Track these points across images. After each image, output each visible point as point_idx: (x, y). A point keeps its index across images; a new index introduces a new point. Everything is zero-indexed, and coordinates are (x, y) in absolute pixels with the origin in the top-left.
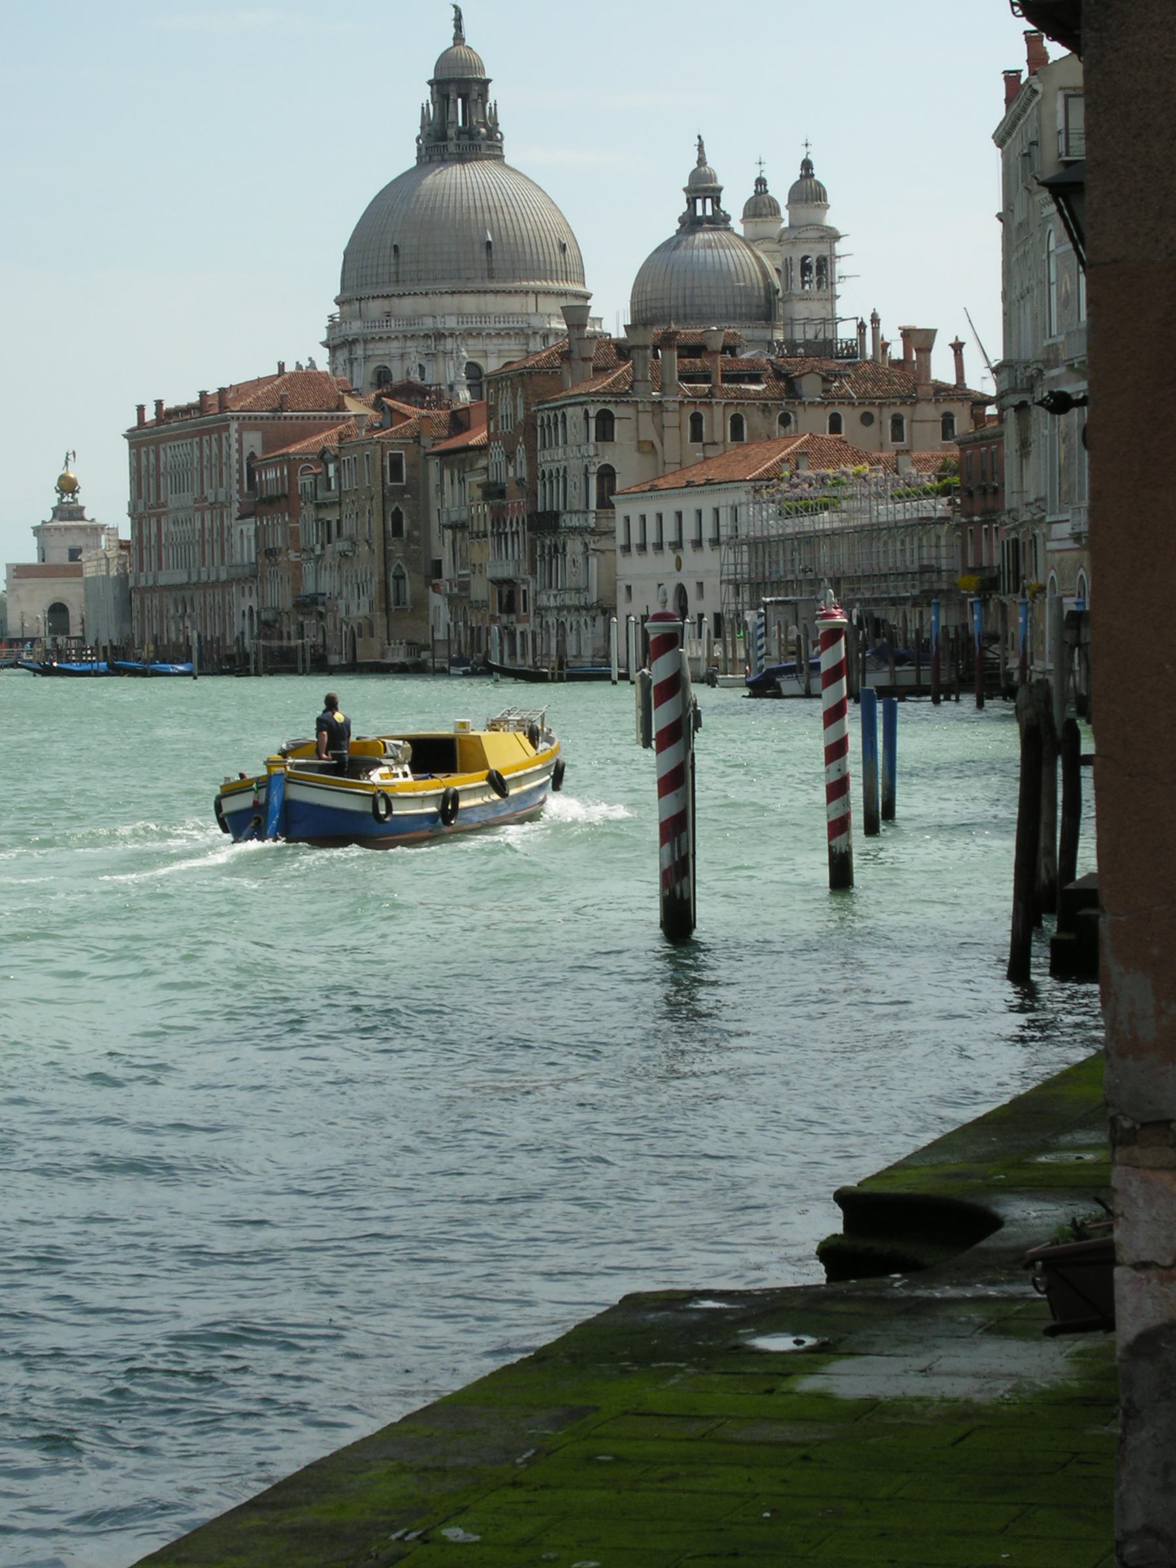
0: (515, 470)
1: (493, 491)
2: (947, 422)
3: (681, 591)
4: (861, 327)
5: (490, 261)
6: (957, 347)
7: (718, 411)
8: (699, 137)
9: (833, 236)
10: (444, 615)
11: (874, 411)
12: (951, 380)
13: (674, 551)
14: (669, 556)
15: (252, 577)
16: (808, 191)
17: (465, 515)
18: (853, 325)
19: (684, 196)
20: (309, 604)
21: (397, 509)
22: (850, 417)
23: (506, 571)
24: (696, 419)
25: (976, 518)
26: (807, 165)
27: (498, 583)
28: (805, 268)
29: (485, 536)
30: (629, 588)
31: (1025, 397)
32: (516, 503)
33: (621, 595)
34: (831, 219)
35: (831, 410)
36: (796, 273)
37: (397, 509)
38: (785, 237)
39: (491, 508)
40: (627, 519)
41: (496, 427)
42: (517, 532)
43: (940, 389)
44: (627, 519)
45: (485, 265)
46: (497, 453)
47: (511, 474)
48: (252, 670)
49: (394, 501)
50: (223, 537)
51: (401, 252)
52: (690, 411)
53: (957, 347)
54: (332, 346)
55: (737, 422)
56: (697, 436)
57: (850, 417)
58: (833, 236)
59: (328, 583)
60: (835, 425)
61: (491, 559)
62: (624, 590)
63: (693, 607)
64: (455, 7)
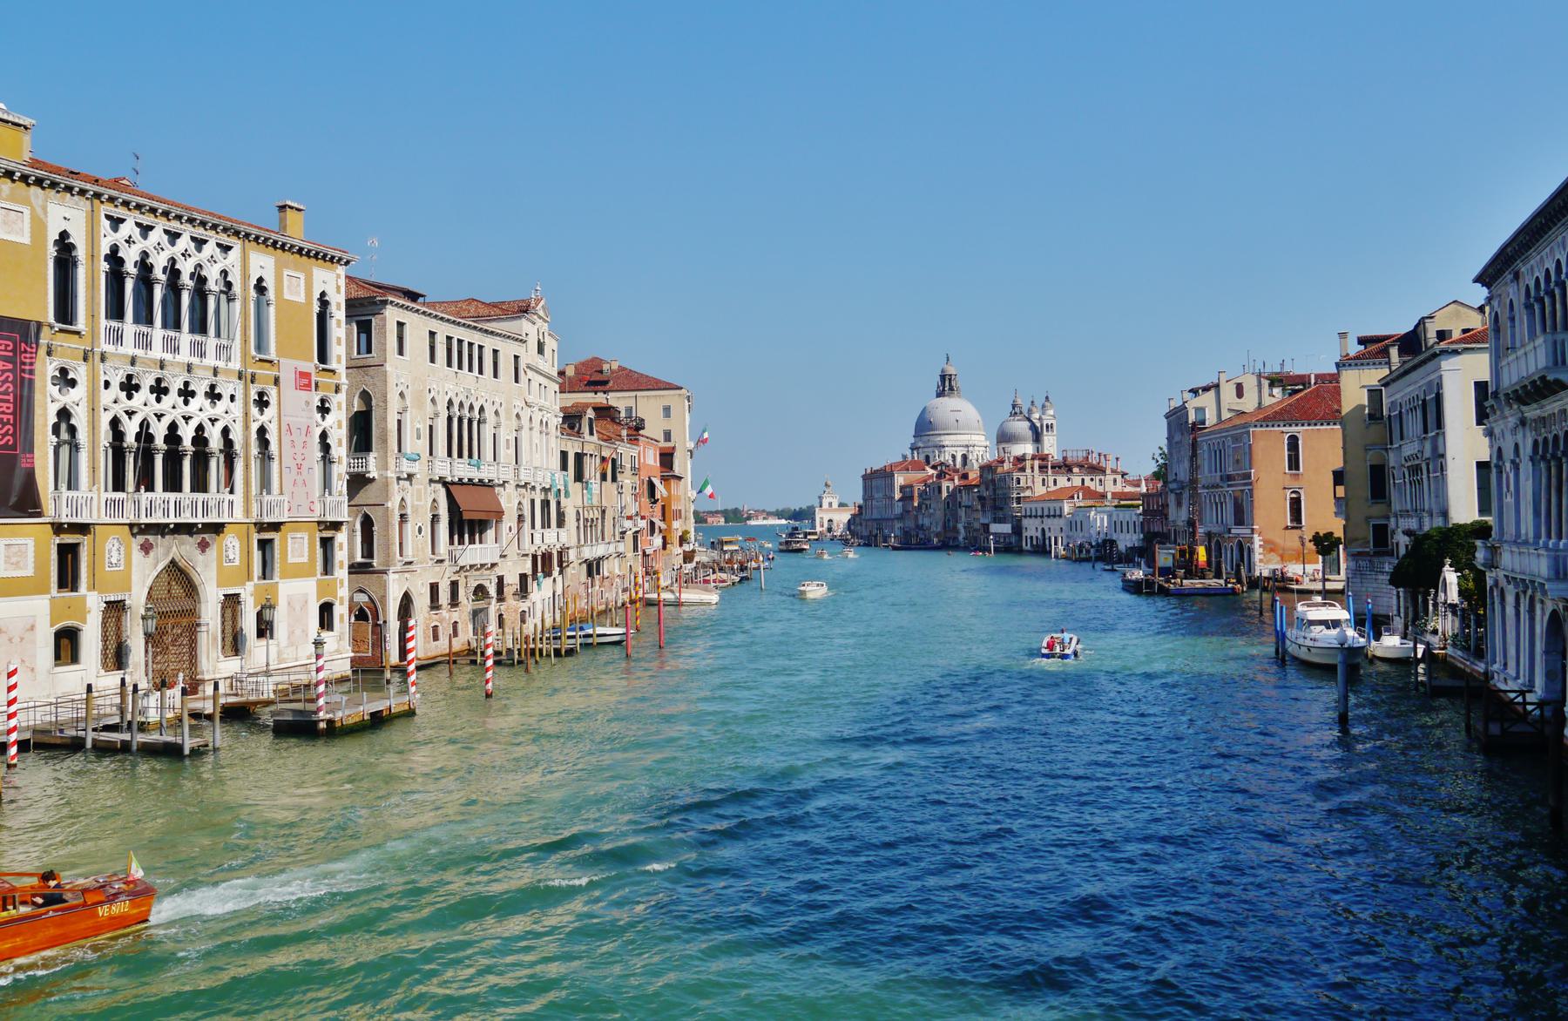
1: (981, 498)
10: (962, 531)
15: (901, 518)
20: (920, 527)
32: (989, 503)
46: (983, 488)
50: (892, 506)
54: (912, 449)
57: (1087, 479)
59: (926, 522)
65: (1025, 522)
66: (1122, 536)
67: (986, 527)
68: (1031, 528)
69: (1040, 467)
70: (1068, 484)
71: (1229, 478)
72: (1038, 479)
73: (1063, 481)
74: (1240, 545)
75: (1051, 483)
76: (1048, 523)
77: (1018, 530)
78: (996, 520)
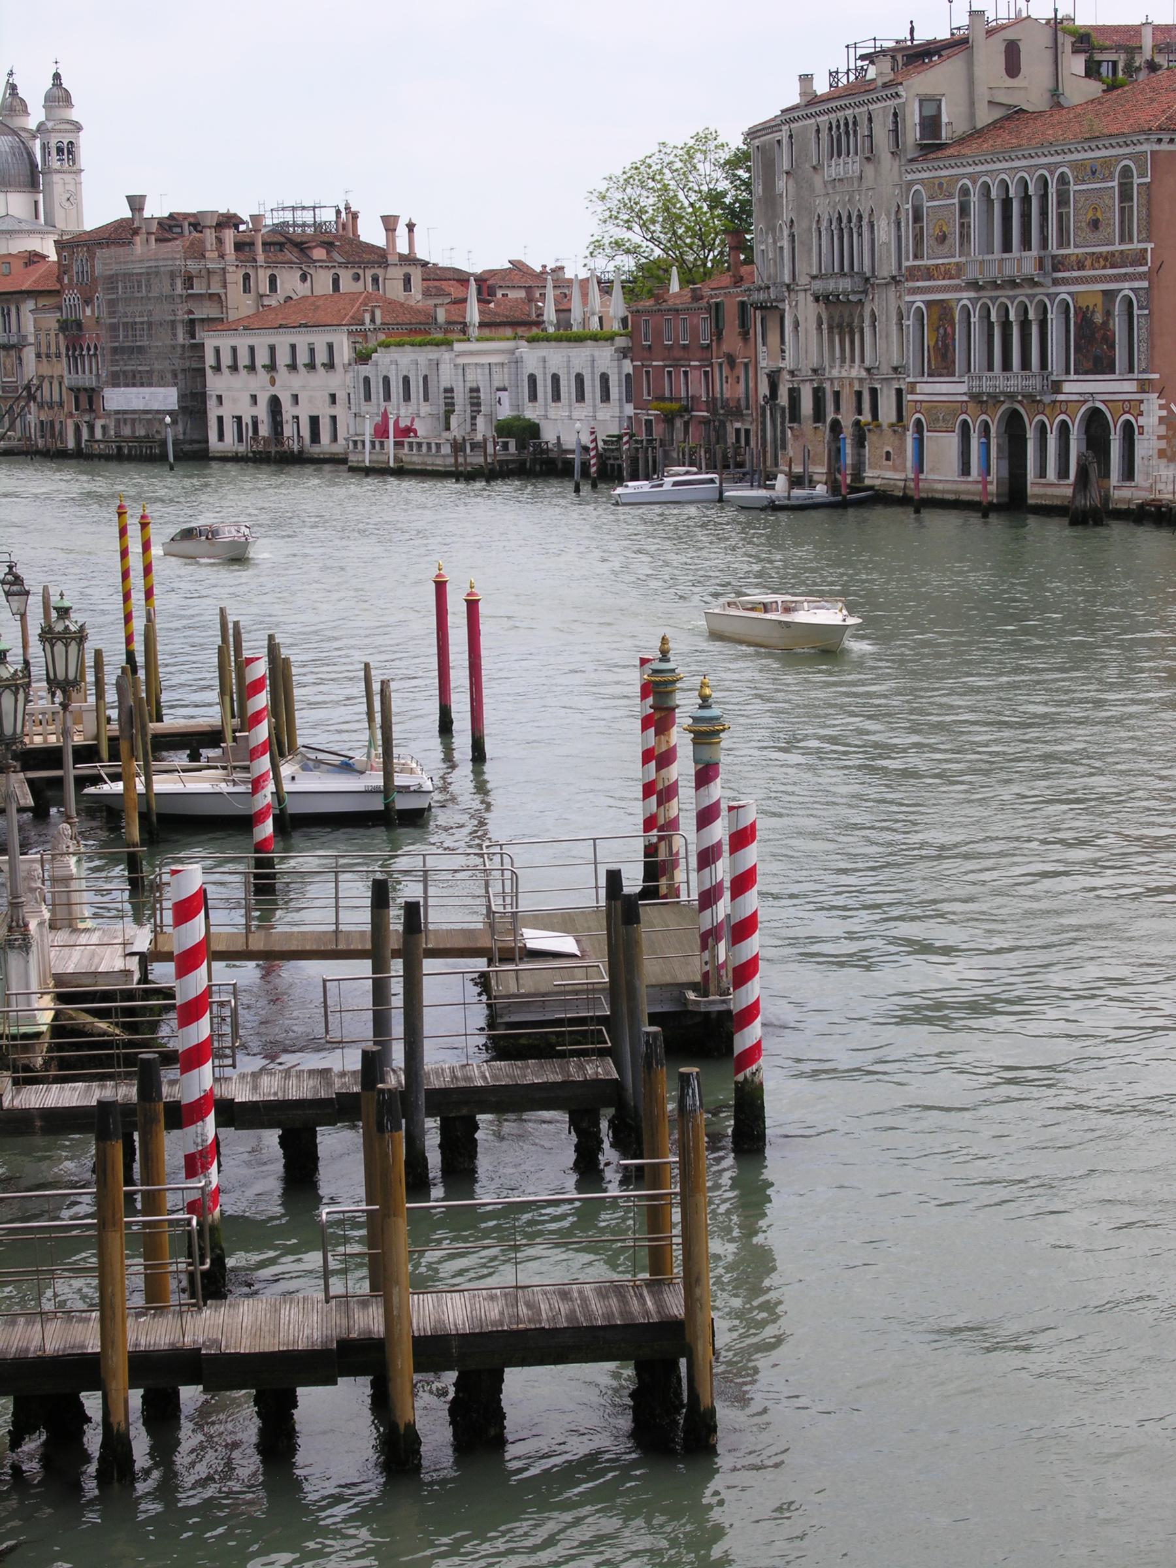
0: (93, 311)
2: (407, 280)
3: (275, 403)
4: (338, 212)
6: (411, 227)
7: (261, 272)
9: (78, 128)
11: (361, 272)
12: (406, 251)
13: (268, 372)
14: (263, 376)
16: (59, 96)
17: (14, 340)
18: (334, 210)
22: (346, 276)
23: (86, 380)
24: (247, 277)
25: (655, 363)
26: (57, 76)
27: (76, 391)
28: (60, 151)
29: (58, 356)
30: (220, 398)
31: (862, 296)
33: (212, 403)
34: (75, 114)
35: (333, 271)
36: (54, 152)
38: (43, 128)
39: (66, 337)
40: (217, 351)
41: (71, 280)
42: (95, 355)
43: (402, 257)
44: (217, 351)
47: (88, 312)
52: (241, 272)
53: (411, 227)
55: (273, 280)
56: (247, 290)
57: (346, 276)
58: (78, 128)
60: (336, 281)
61: (66, 373)
62: (214, 398)
63: (288, 410)
65: (215, 384)
66: (557, 411)
67: (87, 399)
68: (235, 398)
69: (239, 247)
70: (303, 289)
71: (1059, 264)
72: (235, 277)
73: (290, 283)
74: (1096, 423)
75: (265, 288)
76: (286, 384)
77: (194, 405)
78: (116, 380)
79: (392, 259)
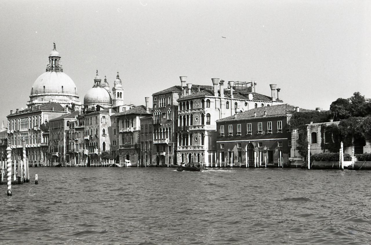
5: (63, 90)
8: (97, 70)
19: (94, 81)
21: (104, 129)
24: (228, 103)
37: (104, 129)
45: (62, 90)
48: (350, 160)
49: (103, 127)
51: (45, 87)
64: (54, 44)
70: (246, 109)
79: (274, 100)
